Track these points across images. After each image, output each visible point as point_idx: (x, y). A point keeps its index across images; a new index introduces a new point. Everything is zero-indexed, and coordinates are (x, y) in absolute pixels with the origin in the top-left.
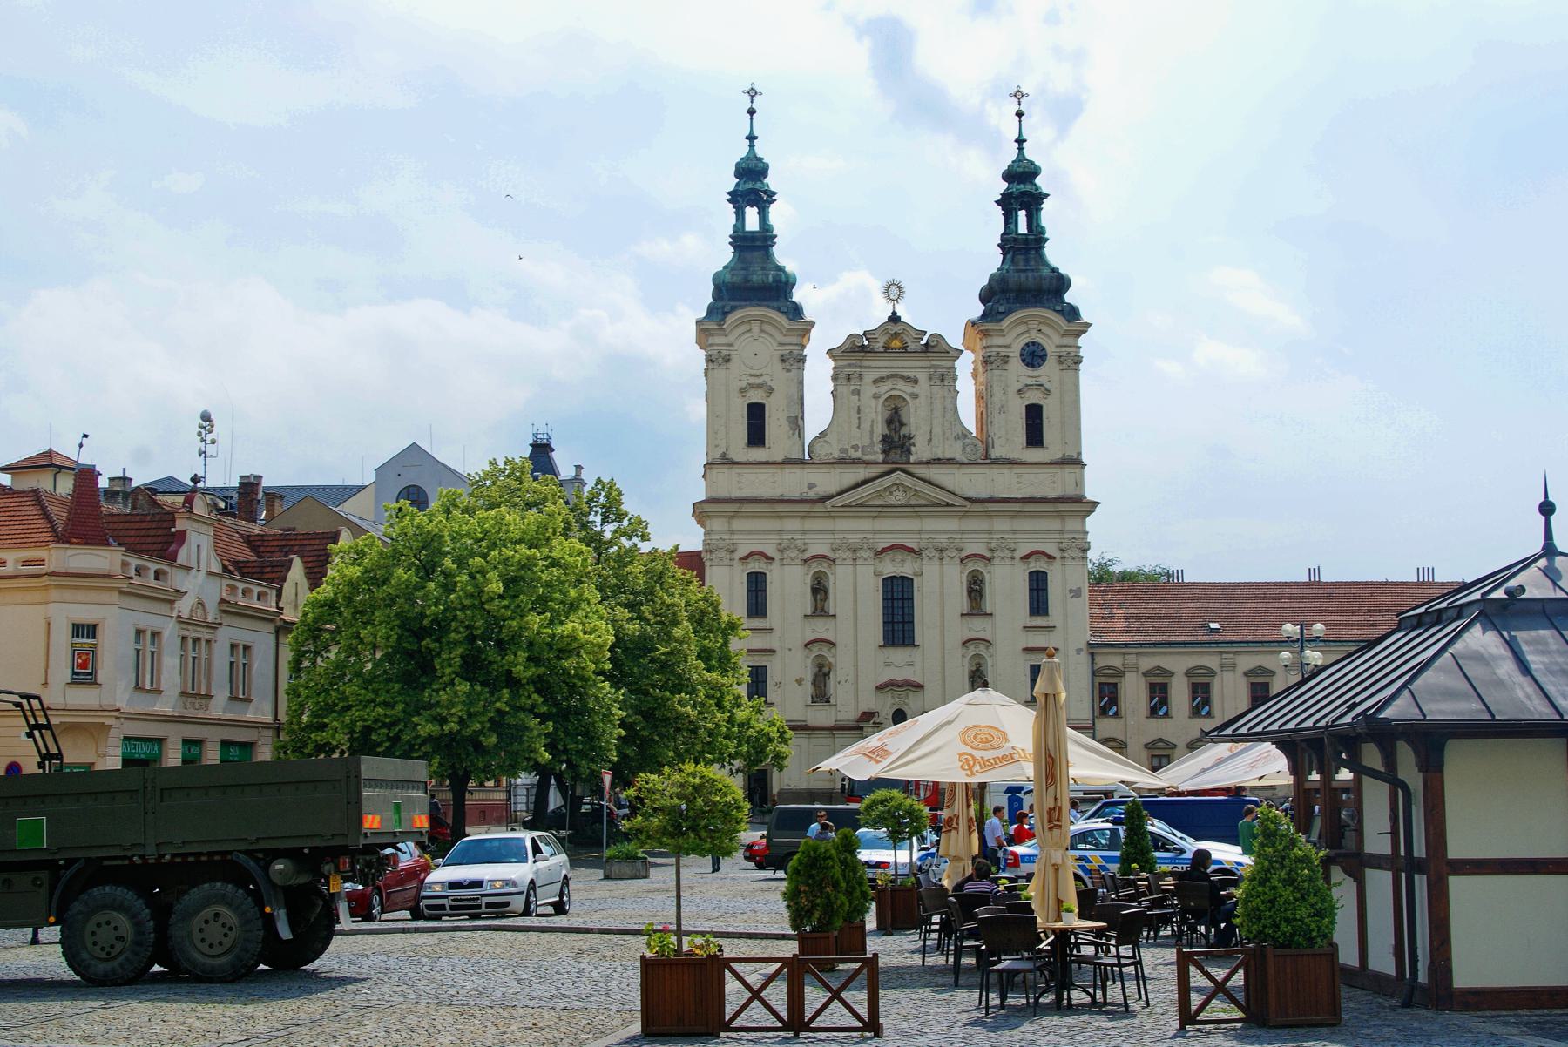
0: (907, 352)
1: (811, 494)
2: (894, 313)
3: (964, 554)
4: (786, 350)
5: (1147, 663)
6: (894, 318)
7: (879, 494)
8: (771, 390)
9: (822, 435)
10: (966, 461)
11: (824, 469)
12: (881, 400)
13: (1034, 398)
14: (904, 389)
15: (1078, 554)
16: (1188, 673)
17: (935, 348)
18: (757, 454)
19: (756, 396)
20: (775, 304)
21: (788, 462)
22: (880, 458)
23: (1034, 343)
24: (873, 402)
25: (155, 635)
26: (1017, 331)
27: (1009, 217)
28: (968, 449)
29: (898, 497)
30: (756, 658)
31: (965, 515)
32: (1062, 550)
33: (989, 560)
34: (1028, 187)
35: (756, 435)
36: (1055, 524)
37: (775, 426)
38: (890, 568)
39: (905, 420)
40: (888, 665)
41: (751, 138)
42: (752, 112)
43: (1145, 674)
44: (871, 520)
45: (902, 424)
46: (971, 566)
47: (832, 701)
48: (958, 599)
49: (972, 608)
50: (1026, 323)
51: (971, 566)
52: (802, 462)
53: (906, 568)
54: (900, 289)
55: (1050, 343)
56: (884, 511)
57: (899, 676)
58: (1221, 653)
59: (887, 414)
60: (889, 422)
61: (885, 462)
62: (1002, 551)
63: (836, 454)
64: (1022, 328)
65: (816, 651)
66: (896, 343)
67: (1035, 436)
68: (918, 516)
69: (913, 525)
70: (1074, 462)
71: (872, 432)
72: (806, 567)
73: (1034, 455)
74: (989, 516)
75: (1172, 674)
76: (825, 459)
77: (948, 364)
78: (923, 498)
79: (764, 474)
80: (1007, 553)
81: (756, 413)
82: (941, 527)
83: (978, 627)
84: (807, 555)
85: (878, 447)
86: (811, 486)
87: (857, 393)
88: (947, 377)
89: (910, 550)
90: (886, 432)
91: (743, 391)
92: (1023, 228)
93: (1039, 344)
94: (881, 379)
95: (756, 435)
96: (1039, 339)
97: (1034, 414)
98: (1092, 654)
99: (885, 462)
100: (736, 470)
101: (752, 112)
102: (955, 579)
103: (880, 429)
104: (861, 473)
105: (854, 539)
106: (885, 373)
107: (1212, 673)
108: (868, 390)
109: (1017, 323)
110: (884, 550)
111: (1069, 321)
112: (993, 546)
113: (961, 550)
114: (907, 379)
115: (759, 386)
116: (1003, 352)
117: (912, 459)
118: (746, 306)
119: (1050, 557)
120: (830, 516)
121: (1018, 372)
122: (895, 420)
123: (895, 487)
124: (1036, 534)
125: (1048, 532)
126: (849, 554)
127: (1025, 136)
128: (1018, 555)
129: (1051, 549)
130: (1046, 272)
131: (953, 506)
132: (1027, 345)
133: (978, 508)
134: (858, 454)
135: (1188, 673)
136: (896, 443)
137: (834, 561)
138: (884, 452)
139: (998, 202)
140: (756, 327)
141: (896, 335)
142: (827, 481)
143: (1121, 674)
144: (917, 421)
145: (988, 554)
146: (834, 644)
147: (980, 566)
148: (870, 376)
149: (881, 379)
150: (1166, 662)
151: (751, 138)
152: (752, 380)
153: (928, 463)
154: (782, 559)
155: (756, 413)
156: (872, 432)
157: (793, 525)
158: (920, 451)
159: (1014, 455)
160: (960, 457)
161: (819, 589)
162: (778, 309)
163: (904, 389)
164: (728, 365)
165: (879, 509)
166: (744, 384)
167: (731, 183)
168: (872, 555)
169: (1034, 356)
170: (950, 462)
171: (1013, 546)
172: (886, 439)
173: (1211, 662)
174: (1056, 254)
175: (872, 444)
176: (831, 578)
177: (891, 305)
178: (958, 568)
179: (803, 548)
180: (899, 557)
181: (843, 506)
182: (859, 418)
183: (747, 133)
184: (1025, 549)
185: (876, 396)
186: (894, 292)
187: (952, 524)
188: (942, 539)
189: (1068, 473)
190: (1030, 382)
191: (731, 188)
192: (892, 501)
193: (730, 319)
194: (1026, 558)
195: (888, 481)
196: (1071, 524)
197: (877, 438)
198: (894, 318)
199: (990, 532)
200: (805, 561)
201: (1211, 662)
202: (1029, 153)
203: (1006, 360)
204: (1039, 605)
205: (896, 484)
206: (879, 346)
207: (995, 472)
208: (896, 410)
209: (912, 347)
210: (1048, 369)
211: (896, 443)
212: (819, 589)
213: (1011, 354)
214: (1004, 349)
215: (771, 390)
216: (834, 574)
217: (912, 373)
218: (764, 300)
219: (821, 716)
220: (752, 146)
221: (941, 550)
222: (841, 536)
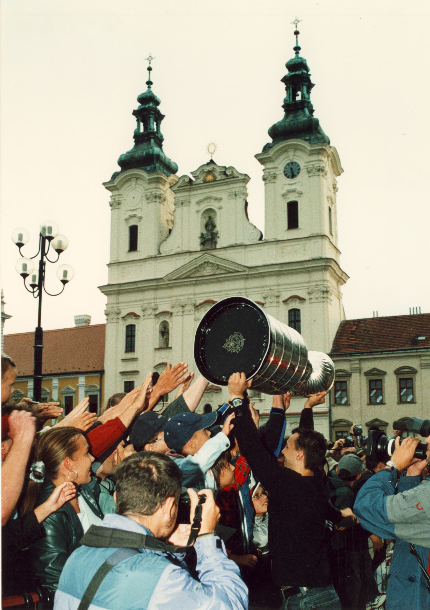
0: (216, 181)
5: (367, 366)
12: (201, 213)
15: (320, 295)
16: (397, 372)
22: (199, 248)
23: (292, 163)
29: (208, 271)
30: (129, 376)
31: (247, 277)
32: (309, 293)
43: (366, 374)
44: (192, 287)
45: (214, 226)
58: (420, 356)
59: (205, 221)
60: (206, 226)
61: (201, 251)
62: (271, 298)
66: (210, 178)
68: (219, 281)
72: (157, 320)
75: (385, 373)
77: (241, 185)
78: (222, 269)
80: (275, 299)
81: (134, 231)
84: (157, 312)
85: (199, 241)
90: (205, 232)
91: (127, 220)
93: (296, 163)
99: (201, 251)
101: (150, 69)
105: (183, 300)
107: (414, 371)
110: (200, 304)
117: (218, 246)
119: (302, 300)
123: (206, 264)
126: (181, 309)
129: (302, 294)
131: (238, 271)
132: (288, 165)
135: (397, 372)
137: (171, 314)
138: (203, 244)
141: (209, 172)
143: (349, 375)
148: (194, 200)
150: (380, 365)
154: (144, 316)
155: (134, 231)
163: (214, 205)
164: (119, 206)
165: (195, 279)
168: (193, 309)
171: (277, 294)
173: (413, 363)
181: (175, 279)
194: (285, 302)
201: (413, 363)
205: (205, 262)
206: (200, 181)
207: (266, 249)
208: (210, 218)
209: (219, 178)
213: (277, 173)
214: (273, 170)
216: (171, 322)
218: (140, 167)
222: (175, 298)
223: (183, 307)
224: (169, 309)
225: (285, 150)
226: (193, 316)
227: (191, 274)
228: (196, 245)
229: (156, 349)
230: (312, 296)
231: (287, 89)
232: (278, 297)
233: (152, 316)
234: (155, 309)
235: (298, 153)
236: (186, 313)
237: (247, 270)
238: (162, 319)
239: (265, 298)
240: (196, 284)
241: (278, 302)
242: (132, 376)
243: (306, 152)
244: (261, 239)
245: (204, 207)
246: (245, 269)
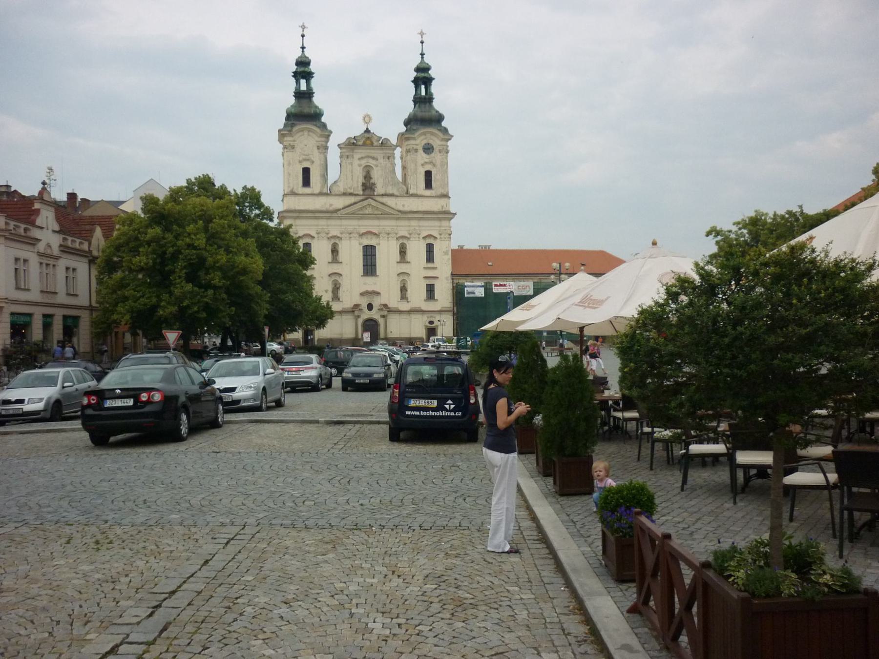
1: (331, 209)
2: (367, 129)
3: (398, 236)
4: (319, 144)
6: (367, 131)
7: (361, 209)
8: (313, 162)
9: (335, 182)
10: (399, 195)
11: (336, 198)
12: (362, 167)
13: (428, 167)
14: (372, 162)
15: (447, 236)
17: (384, 144)
18: (307, 190)
19: (306, 165)
20: (315, 123)
21: (321, 194)
22: (361, 193)
23: (428, 144)
24: (358, 168)
25: (74, 270)
26: (421, 137)
27: (417, 87)
28: (400, 190)
29: (369, 210)
31: (398, 219)
32: (440, 234)
33: (409, 238)
34: (426, 75)
35: (306, 182)
36: (437, 223)
37: (315, 177)
38: (367, 241)
39: (372, 177)
40: (365, 284)
41: (303, 48)
42: (303, 36)
45: (371, 178)
46: (401, 241)
47: (341, 300)
48: (396, 255)
49: (401, 259)
50: (425, 135)
51: (401, 241)
52: (326, 194)
53: (372, 241)
54: (370, 119)
55: (436, 143)
56: (363, 217)
57: (370, 289)
59: (364, 174)
60: (365, 177)
61: (363, 195)
63: (342, 190)
64: (423, 137)
65: (334, 278)
66: (368, 142)
67: (428, 184)
68: (378, 218)
69: (376, 222)
70: (446, 196)
71: (358, 182)
73: (428, 193)
74: (409, 219)
76: (337, 193)
77: (391, 152)
79: (310, 200)
80: (417, 236)
81: (306, 172)
82: (387, 225)
83: (404, 268)
86: (331, 205)
87: (352, 164)
88: (390, 157)
89: (375, 234)
90: (364, 181)
91: (300, 162)
92: (423, 93)
94: (362, 158)
95: (306, 182)
96: (431, 142)
97: (428, 174)
98: (453, 279)
99: (363, 195)
100: (297, 198)
101: (303, 36)
103: (361, 180)
104: (352, 199)
105: (350, 229)
106: (363, 155)
108: (356, 162)
109: (421, 134)
110: (363, 234)
111: (444, 134)
112: (411, 232)
113: (396, 234)
114: (373, 158)
115: (308, 160)
116: (415, 147)
117: (375, 194)
118: (300, 124)
120: (340, 218)
121: (422, 157)
122: (368, 176)
124: (430, 227)
125: (434, 226)
127: (424, 52)
128: (421, 236)
129: (435, 234)
130: (434, 113)
131: (394, 214)
133: (404, 216)
134: (352, 191)
136: (368, 186)
138: (363, 190)
139: (412, 81)
140: (306, 133)
142: (338, 203)
144: (377, 177)
145: (408, 236)
146: (341, 275)
147: (405, 241)
148: (357, 156)
149: (362, 158)
151: (303, 48)
152: (304, 157)
153: (383, 195)
154: (318, 237)
155: (306, 172)
156: (358, 182)
157: (323, 222)
158: (379, 189)
159: (419, 193)
160: (396, 193)
161: (335, 251)
162: (316, 125)
163: (372, 162)
166: (301, 159)
167: (294, 68)
169: (428, 149)
170: (392, 195)
171: (419, 232)
172: (364, 185)
174: (438, 105)
175: (358, 187)
176: (340, 246)
177: (366, 125)
178: (395, 242)
179: (328, 232)
180: (369, 236)
182: (352, 175)
183: (301, 45)
184: (424, 234)
185: (360, 165)
186: (367, 119)
187: (393, 223)
188: (388, 229)
189: (442, 202)
190: (427, 160)
191: (294, 70)
192: (367, 212)
193: (295, 129)
194: (424, 238)
195: (365, 203)
196: (445, 223)
197: (360, 184)
198: (367, 131)
199: (410, 226)
200: (328, 238)
202: (426, 60)
203: (416, 151)
204: (430, 258)
206: (361, 143)
207: (411, 200)
209: (375, 144)
210: (436, 156)
211: (368, 186)
212: (335, 251)
215: (313, 162)
217: (375, 155)
220: (303, 51)
221: (388, 234)
223: (350, 234)
224: (339, 235)
225: (424, 134)
226: (358, 241)
229: (329, 262)
230: (442, 236)
232: (419, 234)
233: (326, 239)
234: (328, 234)
235: (432, 137)
236: (352, 239)
237: (400, 214)
238: (333, 241)
239: (410, 234)
240: (361, 218)
241: (419, 238)
243: (438, 138)
245: (364, 162)
246: (397, 213)
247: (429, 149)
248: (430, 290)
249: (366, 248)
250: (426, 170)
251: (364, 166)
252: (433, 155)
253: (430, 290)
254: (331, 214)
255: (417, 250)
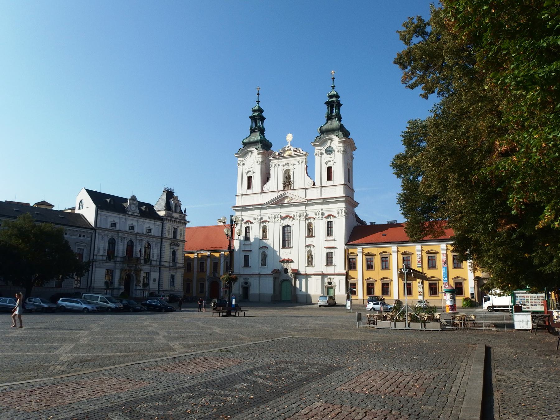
16: (381, 254)
30: (246, 253)
47: (267, 266)
83: (309, 241)
102: (303, 225)
108: (281, 168)
117: (292, 188)
138: (284, 187)
163: (291, 167)
219: (265, 271)
227: (279, 202)
228: (281, 187)
231: (328, 107)
242: (248, 253)
244: (314, 185)
247: (329, 151)
248: (329, 257)
249: (284, 228)
250: (328, 166)
251: (285, 170)
252: (332, 155)
253: (329, 257)
254: (261, 207)
255: (319, 227)
